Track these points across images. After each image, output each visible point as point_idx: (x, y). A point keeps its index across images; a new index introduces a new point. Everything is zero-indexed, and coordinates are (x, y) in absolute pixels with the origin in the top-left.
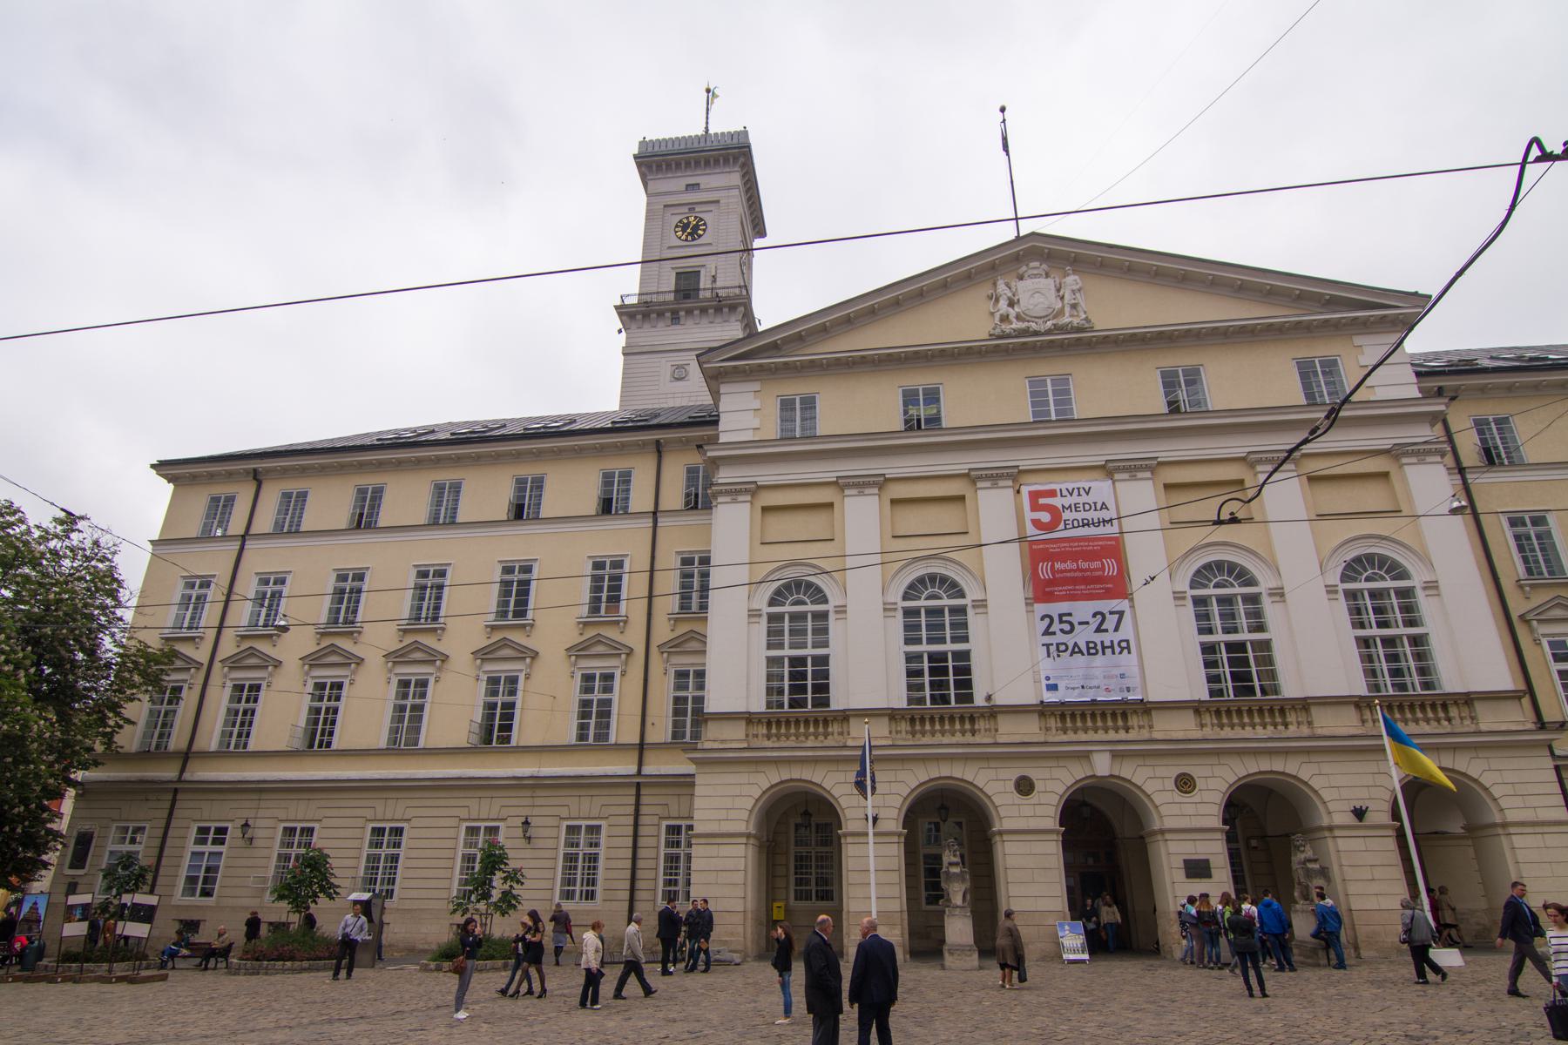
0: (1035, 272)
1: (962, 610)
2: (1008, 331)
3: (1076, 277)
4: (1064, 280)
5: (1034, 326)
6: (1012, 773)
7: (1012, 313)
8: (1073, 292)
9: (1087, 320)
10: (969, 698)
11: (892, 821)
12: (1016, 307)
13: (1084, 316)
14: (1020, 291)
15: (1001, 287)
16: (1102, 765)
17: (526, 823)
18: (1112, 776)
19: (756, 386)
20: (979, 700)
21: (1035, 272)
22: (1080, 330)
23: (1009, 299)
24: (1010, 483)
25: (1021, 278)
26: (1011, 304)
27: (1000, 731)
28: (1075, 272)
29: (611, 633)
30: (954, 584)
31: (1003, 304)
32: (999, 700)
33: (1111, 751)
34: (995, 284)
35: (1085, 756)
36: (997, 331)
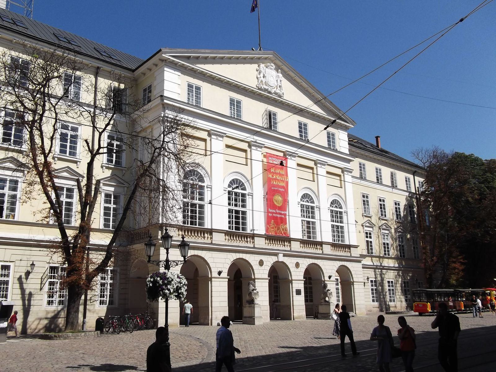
0: (272, 67)
5: (270, 90)
7: (264, 80)
9: (283, 93)
10: (244, 229)
11: (225, 274)
12: (265, 78)
14: (267, 73)
16: (281, 258)
17: (33, 265)
21: (272, 67)
22: (280, 96)
23: (264, 75)
26: (264, 77)
29: (73, 166)
31: (262, 75)
32: (255, 232)
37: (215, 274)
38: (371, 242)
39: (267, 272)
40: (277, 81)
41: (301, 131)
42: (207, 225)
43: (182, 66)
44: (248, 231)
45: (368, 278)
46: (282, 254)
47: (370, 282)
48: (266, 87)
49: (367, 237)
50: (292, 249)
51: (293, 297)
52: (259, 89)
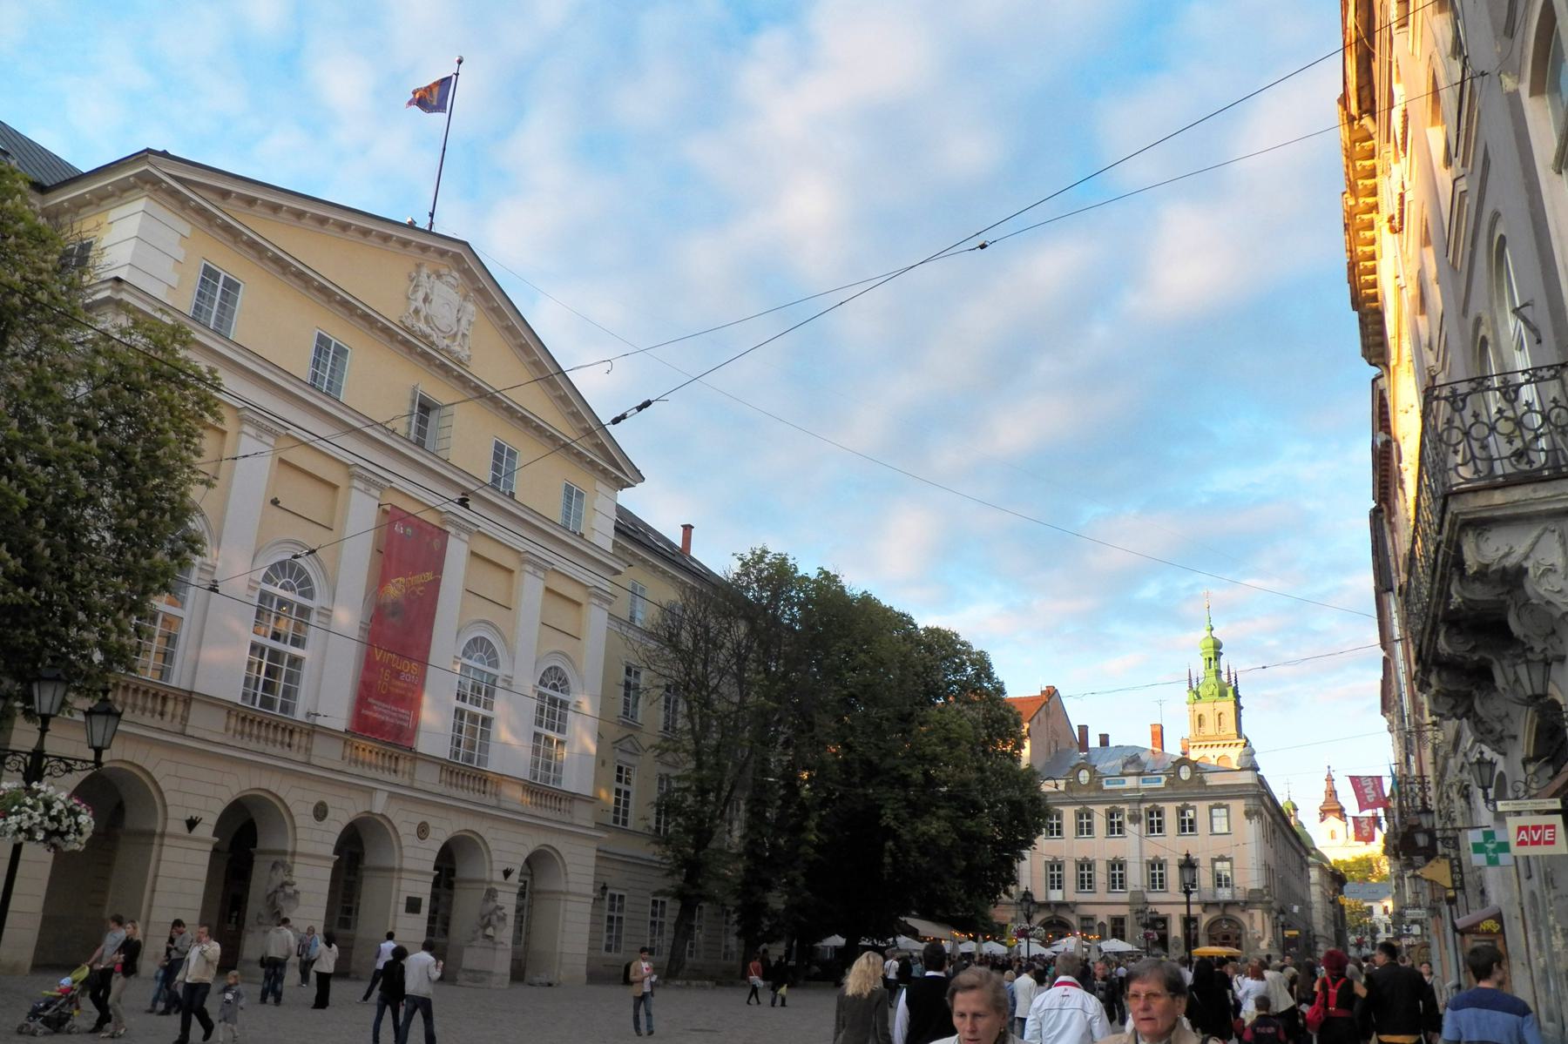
0: (452, 281)
1: (304, 611)
2: (417, 328)
3: (474, 308)
4: (465, 304)
5: (434, 338)
6: (315, 799)
8: (470, 323)
11: (206, 830)
13: (468, 353)
15: (425, 271)
16: (379, 804)
18: (382, 815)
19: (186, 229)
20: (299, 715)
22: (460, 362)
23: (427, 294)
24: (377, 493)
25: (439, 276)
26: (426, 299)
27: (315, 752)
28: (475, 302)
30: (308, 581)
31: (420, 295)
32: (320, 721)
33: (390, 792)
34: (419, 266)
35: (371, 791)
36: (408, 323)
37: (176, 826)
38: (627, 794)
39: (334, 839)
40: (459, 320)
41: (496, 468)
42: (178, 679)
43: (201, 211)
44: (299, 715)
45: (604, 888)
46: (386, 794)
47: (607, 898)
48: (428, 331)
49: (619, 779)
50: (417, 785)
51: (396, 916)
52: (407, 330)
